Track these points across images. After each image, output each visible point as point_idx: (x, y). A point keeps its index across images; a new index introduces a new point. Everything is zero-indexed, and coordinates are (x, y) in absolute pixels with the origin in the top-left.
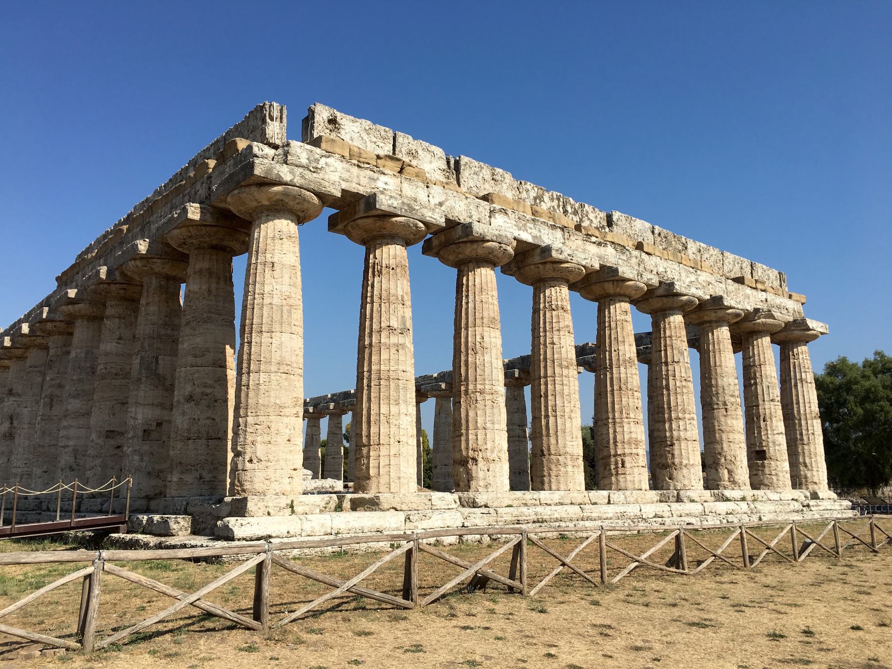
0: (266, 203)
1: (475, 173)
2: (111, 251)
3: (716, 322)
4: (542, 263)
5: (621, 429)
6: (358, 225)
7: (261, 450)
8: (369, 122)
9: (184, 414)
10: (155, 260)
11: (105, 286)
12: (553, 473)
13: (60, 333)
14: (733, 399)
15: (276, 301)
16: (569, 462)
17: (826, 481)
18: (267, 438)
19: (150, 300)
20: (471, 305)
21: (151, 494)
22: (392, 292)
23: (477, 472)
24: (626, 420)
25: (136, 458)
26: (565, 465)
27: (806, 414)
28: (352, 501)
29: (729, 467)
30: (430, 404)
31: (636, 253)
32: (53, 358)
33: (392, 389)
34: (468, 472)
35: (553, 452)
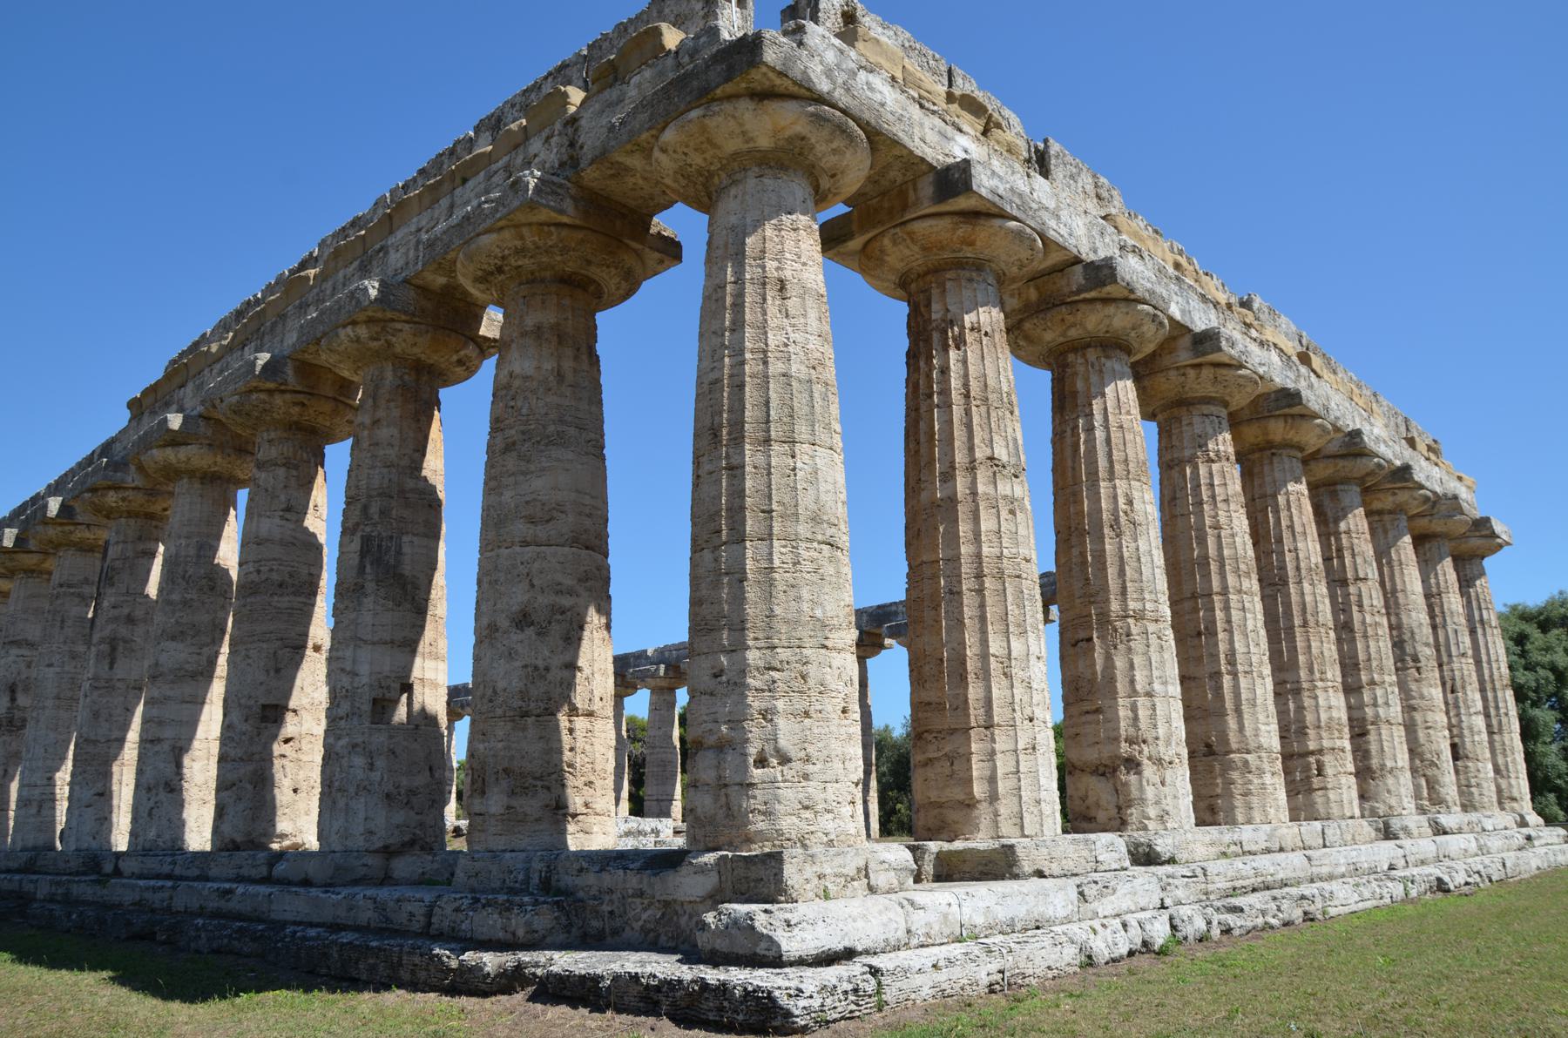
0: (764, 143)
1: (1072, 177)
2: (274, 325)
3: (1390, 512)
4: (1194, 366)
5: (1312, 702)
6: (911, 234)
7: (787, 733)
8: (908, 35)
9: (511, 655)
10: (398, 326)
11: (263, 396)
12: (1237, 790)
13: (130, 514)
15: (795, 368)
17: (1529, 796)
18: (800, 704)
19: (381, 413)
20: (1099, 434)
21: (394, 841)
22: (991, 382)
23: (1141, 789)
24: (1319, 684)
25: (359, 761)
26: (1261, 772)
27: (1493, 681)
29: (1429, 772)
30: (893, 661)
31: (1303, 370)
32: (118, 564)
33: (1010, 598)
34: (1119, 790)
35: (1234, 746)
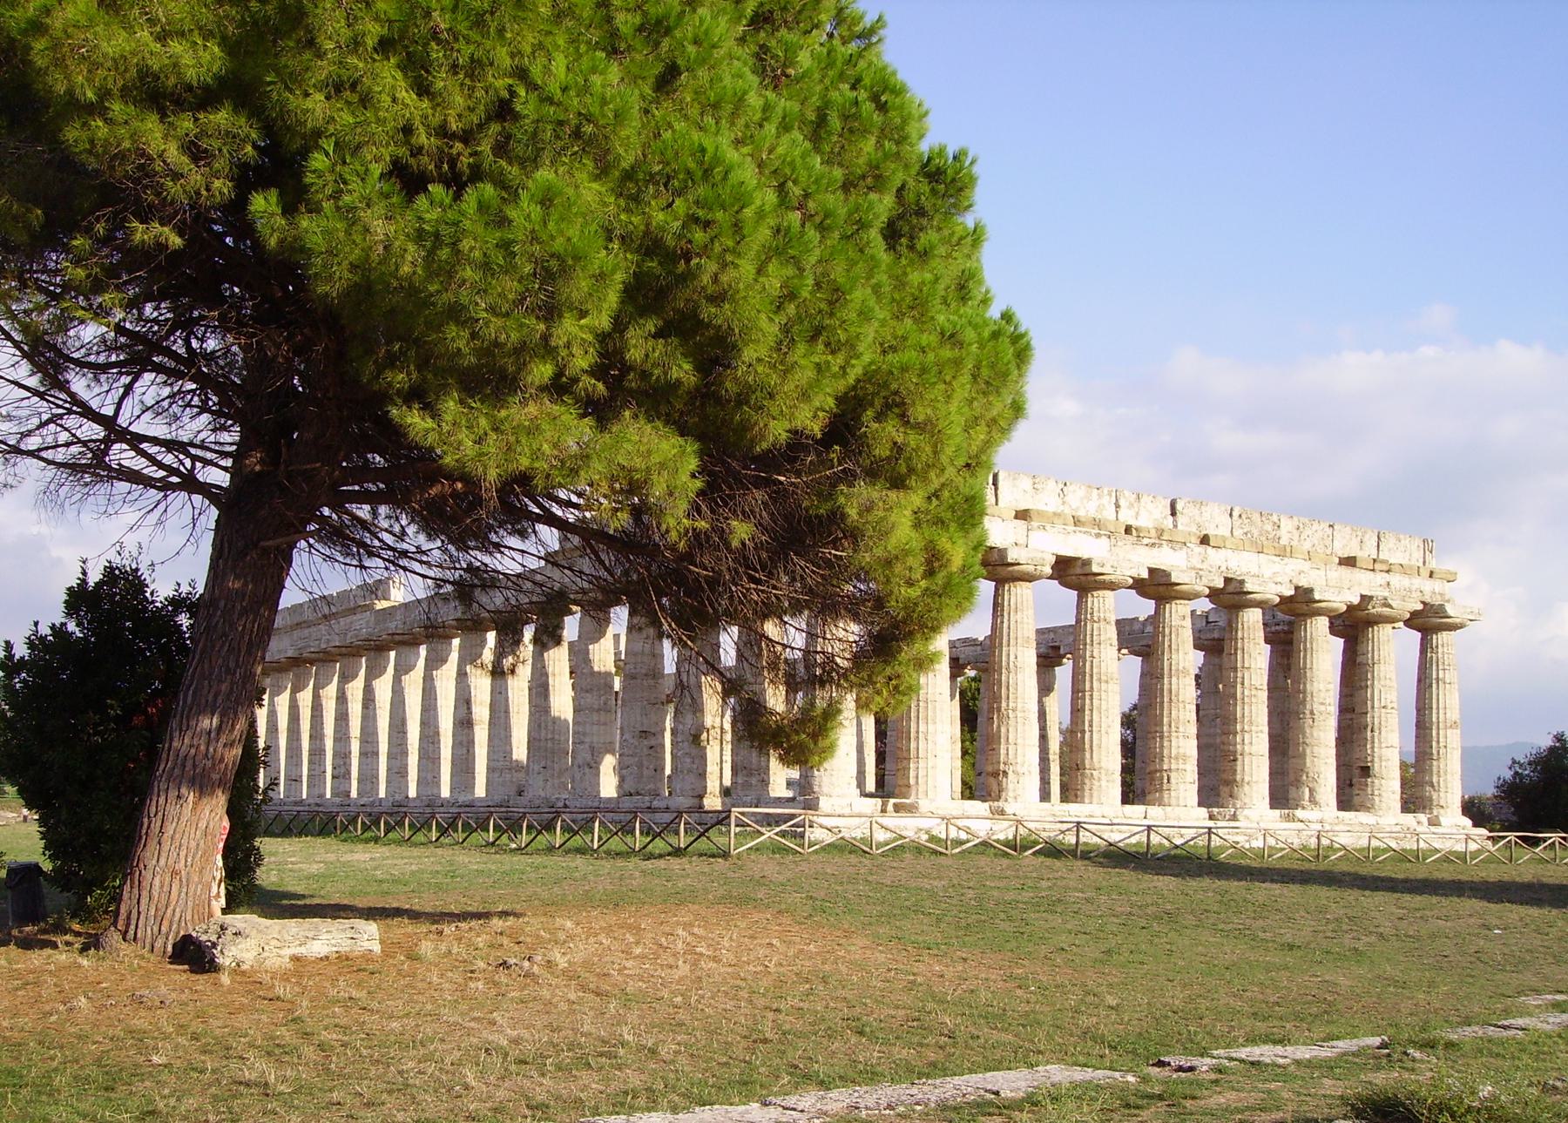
12: (1087, 788)
14: (1322, 708)
16: (1103, 777)
28: (895, 805)
